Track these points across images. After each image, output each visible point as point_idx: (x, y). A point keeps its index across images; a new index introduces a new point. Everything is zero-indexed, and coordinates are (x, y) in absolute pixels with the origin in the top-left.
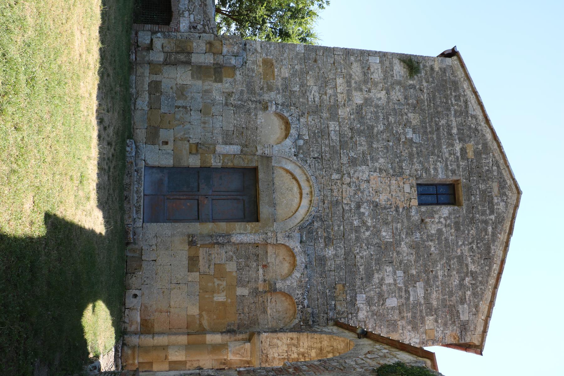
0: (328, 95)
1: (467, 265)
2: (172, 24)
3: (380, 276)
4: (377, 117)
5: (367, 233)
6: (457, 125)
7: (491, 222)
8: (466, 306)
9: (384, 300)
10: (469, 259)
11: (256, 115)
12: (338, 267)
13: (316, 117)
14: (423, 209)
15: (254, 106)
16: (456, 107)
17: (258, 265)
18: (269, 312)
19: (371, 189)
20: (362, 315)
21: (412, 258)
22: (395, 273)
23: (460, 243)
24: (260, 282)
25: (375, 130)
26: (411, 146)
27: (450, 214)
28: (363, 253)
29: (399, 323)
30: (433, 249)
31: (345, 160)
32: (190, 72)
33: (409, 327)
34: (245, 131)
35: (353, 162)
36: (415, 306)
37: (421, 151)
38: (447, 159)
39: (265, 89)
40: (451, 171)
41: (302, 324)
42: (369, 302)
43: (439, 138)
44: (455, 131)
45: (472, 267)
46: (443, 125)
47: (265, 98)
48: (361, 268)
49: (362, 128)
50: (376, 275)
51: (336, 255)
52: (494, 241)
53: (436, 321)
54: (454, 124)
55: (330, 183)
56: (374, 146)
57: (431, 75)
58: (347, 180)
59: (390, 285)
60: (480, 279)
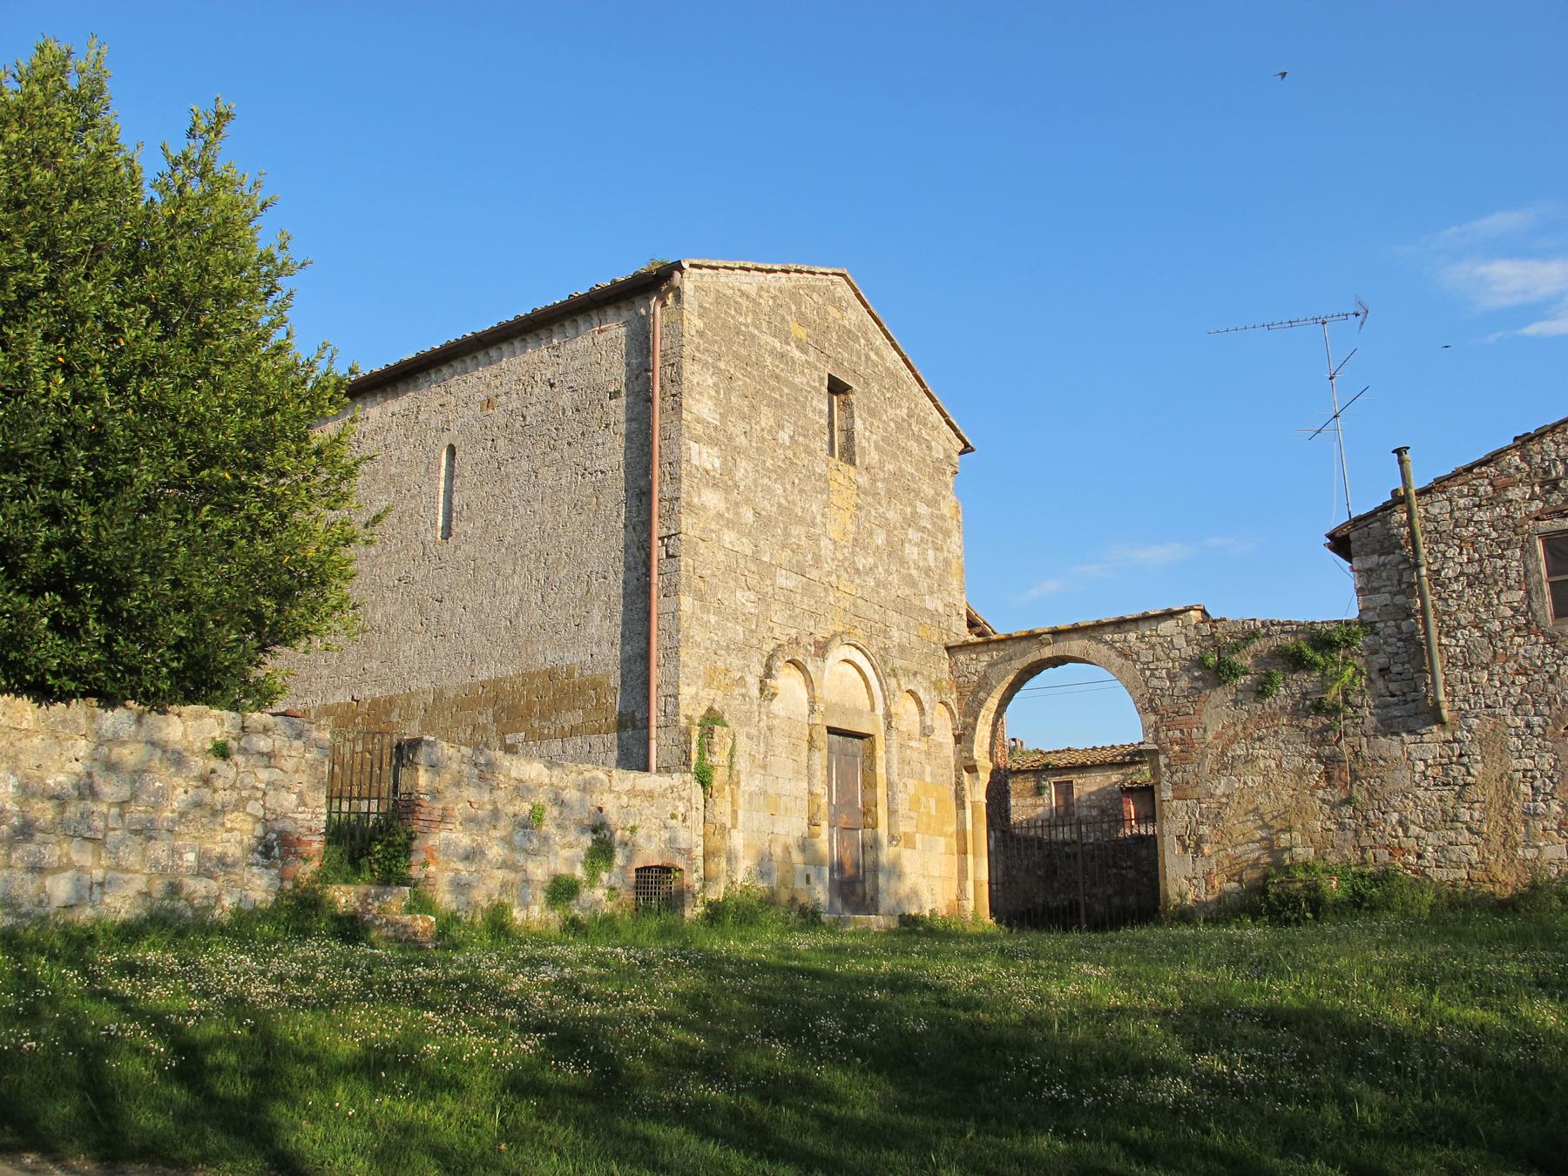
14: (858, 462)
31: (814, 574)
35: (817, 559)
36: (934, 524)
54: (770, 339)
58: (833, 578)
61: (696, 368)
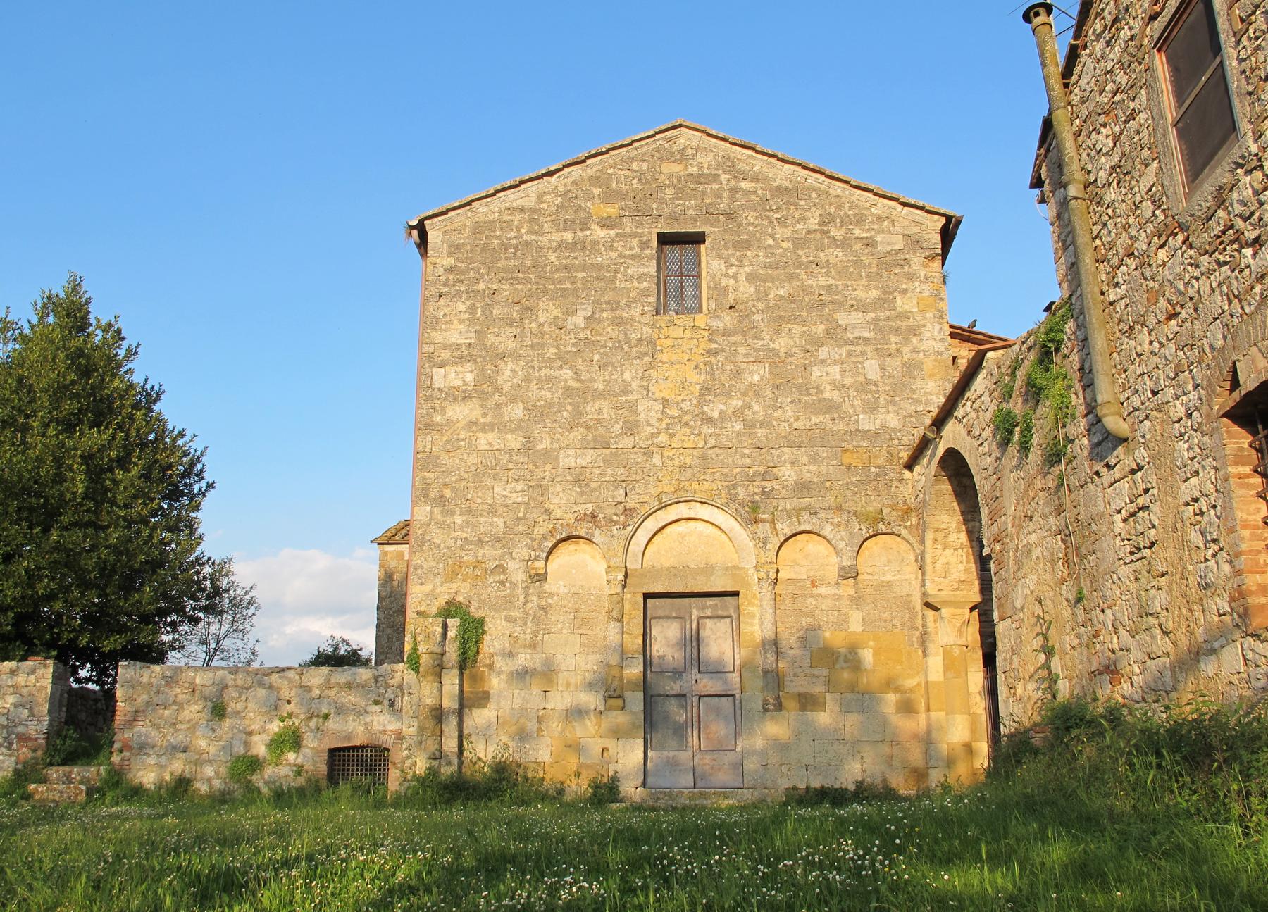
0: (511, 466)
1: (809, 232)
2: (387, 740)
3: (829, 387)
4: (549, 379)
5: (756, 407)
6: (558, 231)
7: (733, 182)
8: (878, 239)
9: (868, 381)
10: (799, 227)
11: (551, 595)
12: (814, 460)
13: (551, 490)
15: (535, 599)
16: (523, 231)
17: (812, 595)
18: (888, 577)
19: (679, 398)
20: (894, 422)
21: (798, 329)
22: (823, 362)
23: (771, 241)
24: (840, 591)
25: (571, 383)
26: (599, 320)
27: (720, 257)
28: (790, 415)
29: (906, 357)
30: (782, 292)
31: (627, 441)
33: (915, 340)
34: (580, 615)
35: (631, 427)
36: (879, 329)
37: (608, 302)
38: (620, 256)
40: (642, 249)
41: (908, 524)
42: (871, 408)
43: (584, 268)
44: (569, 236)
45: (813, 223)
46: (558, 258)
48: (814, 420)
49: (569, 408)
50: (827, 395)
51: (794, 463)
52: (766, 179)
53: (904, 292)
54: (556, 237)
55: (670, 469)
56: (601, 387)
57: (463, 273)
58: (663, 438)
59: (843, 371)
60: (832, 209)
61: (442, 302)
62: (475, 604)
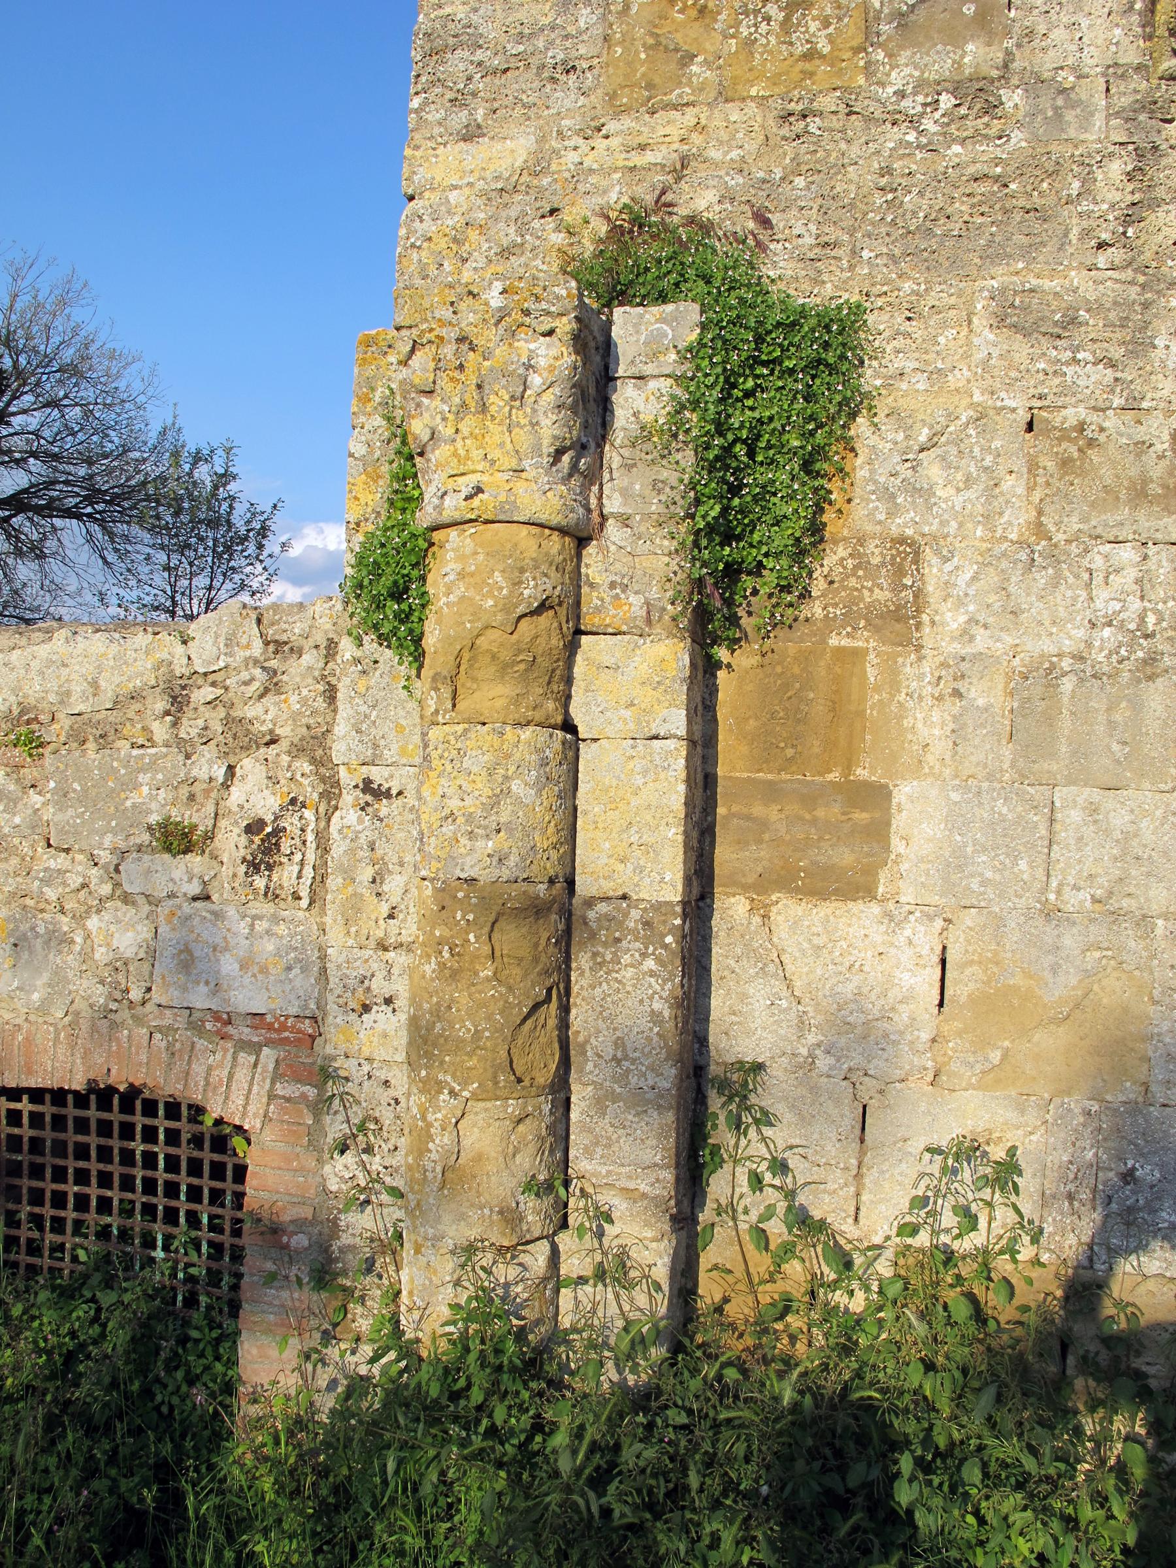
32: (788, 911)
39: (975, 54)
47: (1093, 60)
62: (797, 229)
